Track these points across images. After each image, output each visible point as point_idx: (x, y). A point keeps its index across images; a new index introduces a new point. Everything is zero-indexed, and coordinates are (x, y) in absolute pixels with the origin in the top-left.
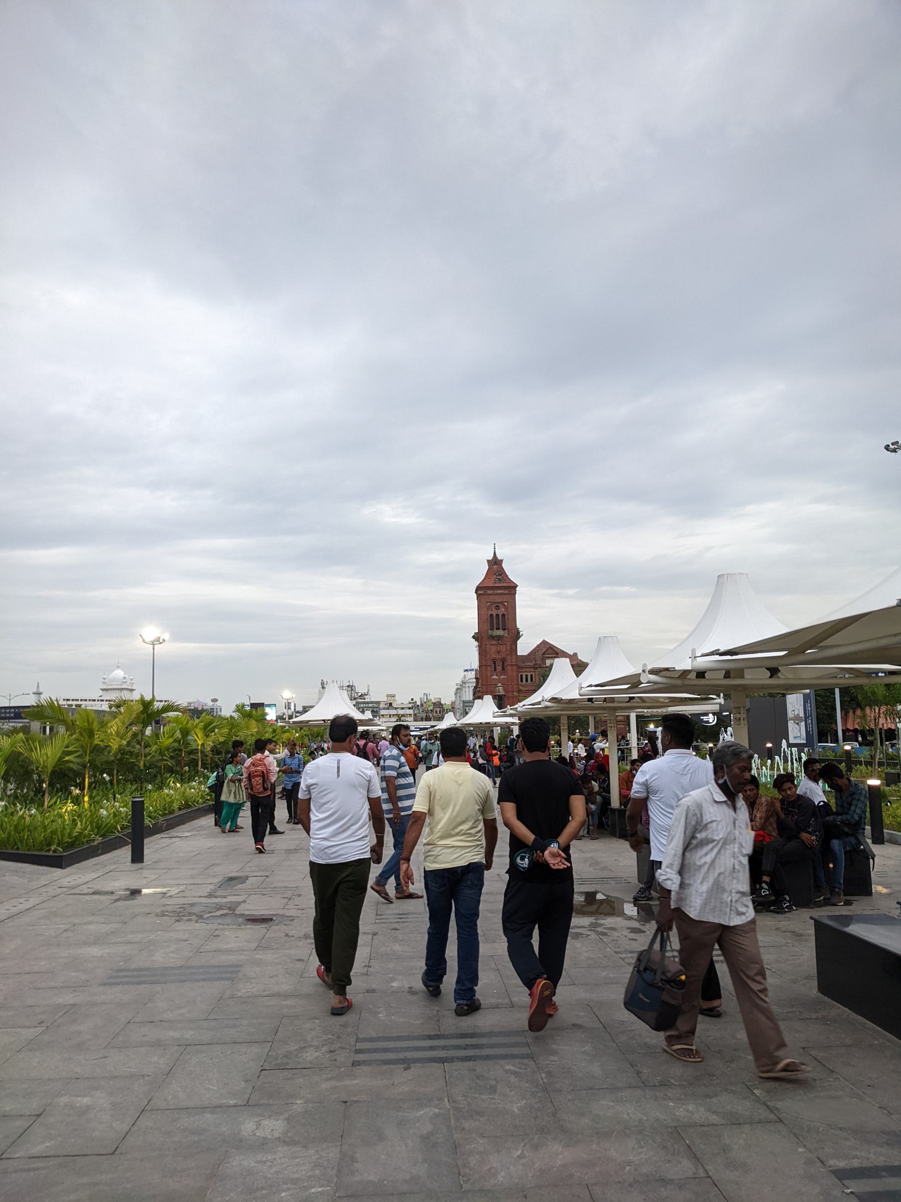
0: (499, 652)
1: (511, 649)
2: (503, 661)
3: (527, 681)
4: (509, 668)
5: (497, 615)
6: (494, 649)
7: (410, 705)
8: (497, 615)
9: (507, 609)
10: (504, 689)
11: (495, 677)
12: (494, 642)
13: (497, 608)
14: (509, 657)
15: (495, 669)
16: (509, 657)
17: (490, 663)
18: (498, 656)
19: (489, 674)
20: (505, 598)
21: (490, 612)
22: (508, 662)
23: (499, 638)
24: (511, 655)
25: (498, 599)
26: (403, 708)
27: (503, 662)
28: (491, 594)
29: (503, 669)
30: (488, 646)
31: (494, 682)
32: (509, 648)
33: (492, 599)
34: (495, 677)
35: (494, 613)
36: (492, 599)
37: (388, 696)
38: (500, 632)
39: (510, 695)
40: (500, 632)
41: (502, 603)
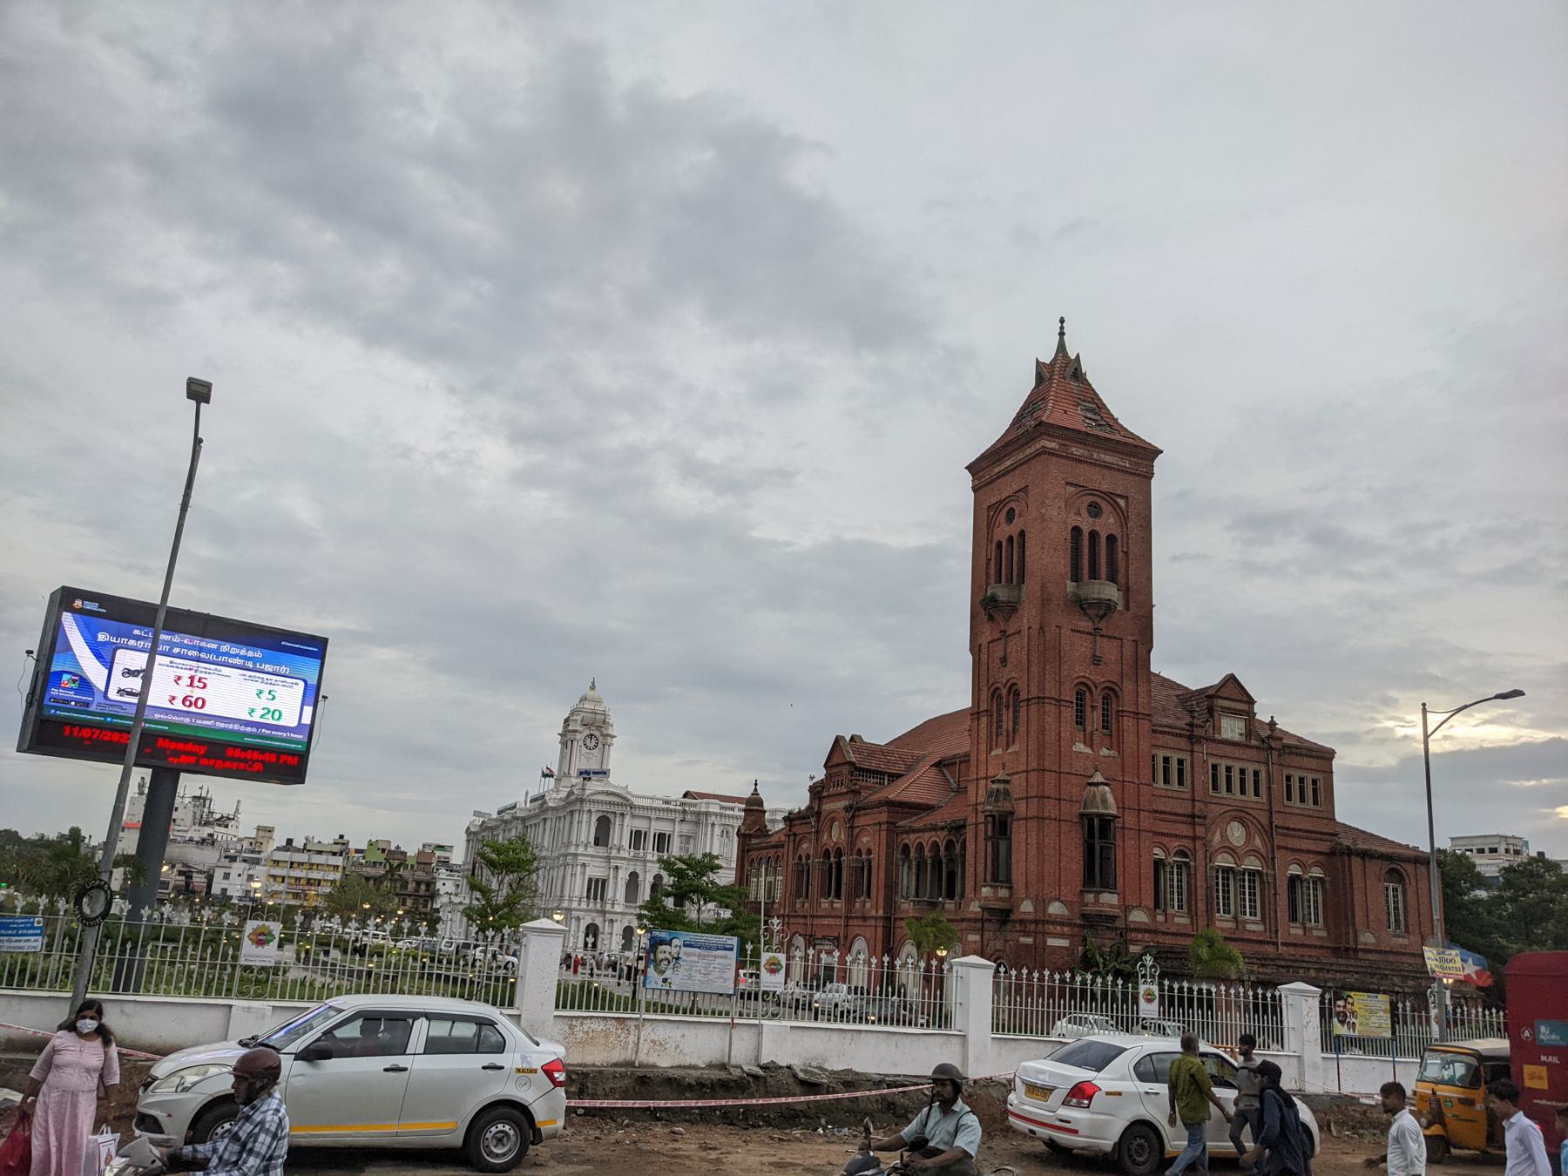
2: (1111, 693)
5: (1093, 535)
7: (337, 848)
9: (1123, 518)
11: (1080, 747)
12: (1085, 625)
16: (1128, 686)
18: (1098, 676)
19: (1066, 735)
26: (320, 852)
30: (1066, 632)
33: (1084, 474)
35: (1086, 524)
37: (259, 828)
38: (1111, 592)
40: (1111, 592)
41: (1110, 497)
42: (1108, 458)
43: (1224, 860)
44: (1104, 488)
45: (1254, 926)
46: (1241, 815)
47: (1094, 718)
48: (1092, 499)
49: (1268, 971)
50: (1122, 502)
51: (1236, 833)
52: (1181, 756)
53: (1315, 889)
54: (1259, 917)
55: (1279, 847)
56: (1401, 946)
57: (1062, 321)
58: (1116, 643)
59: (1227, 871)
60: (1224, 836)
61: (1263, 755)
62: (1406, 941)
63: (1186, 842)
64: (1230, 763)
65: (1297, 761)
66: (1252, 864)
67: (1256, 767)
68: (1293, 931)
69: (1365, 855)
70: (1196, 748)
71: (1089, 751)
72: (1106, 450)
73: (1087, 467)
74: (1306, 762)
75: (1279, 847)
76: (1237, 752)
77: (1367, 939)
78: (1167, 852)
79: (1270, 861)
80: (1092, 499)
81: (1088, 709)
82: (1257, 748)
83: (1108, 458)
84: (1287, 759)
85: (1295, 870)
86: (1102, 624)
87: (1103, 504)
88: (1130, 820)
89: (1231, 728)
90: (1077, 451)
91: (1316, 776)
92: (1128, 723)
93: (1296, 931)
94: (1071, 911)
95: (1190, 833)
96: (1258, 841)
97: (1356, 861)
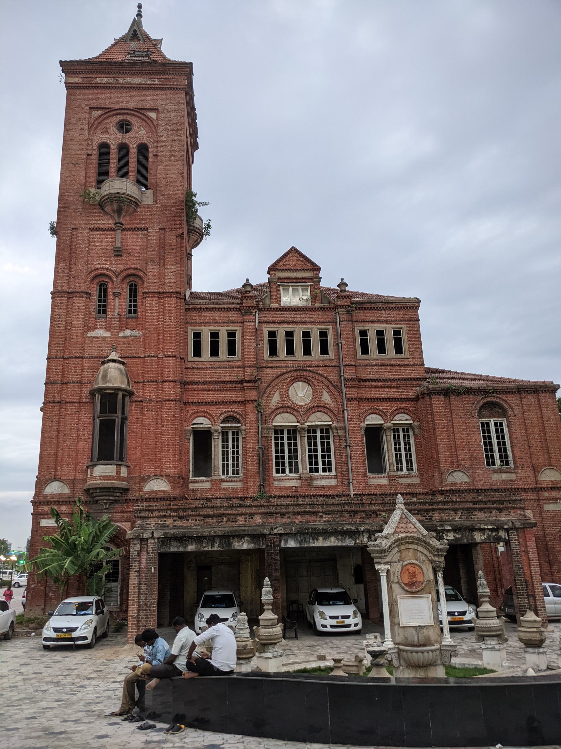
0: (118, 252)
1: (163, 245)
2: (134, 281)
3: (215, 352)
4: (151, 303)
5: (123, 148)
6: (103, 242)
8: (123, 148)
9: (153, 126)
10: (128, 375)
11: (100, 333)
12: (106, 222)
13: (124, 127)
14: (153, 269)
15: (102, 308)
16: (153, 269)
17: (82, 284)
20: (149, 99)
21: (99, 138)
22: (151, 283)
23: (121, 204)
24: (161, 260)
25: (131, 101)
27: (133, 289)
28: (104, 87)
29: (133, 308)
30: (83, 233)
31: (92, 350)
32: (154, 237)
34: (100, 333)
35: (114, 139)
36: (110, 99)
38: (126, 186)
39: (150, 392)
40: (126, 186)
41: (140, 112)
42: (136, 81)
43: (284, 420)
44: (132, 105)
45: (324, 481)
46: (302, 374)
47: (117, 305)
48: (120, 117)
49: (191, 522)
50: (153, 115)
51: (301, 393)
52: (232, 328)
53: (406, 437)
54: (334, 473)
55: (348, 399)
56: (505, 482)
57: (140, 6)
58: (140, 234)
59: (293, 431)
60: (285, 395)
61: (329, 315)
62: (513, 477)
63: (235, 408)
64: (289, 328)
65: (371, 315)
66: (319, 419)
67: (323, 327)
68: (373, 482)
69: (447, 392)
70: (247, 318)
71: (108, 334)
72: (134, 74)
73: (113, 92)
74: (384, 314)
75: (348, 399)
76: (299, 316)
77: (458, 479)
78: (213, 421)
79: (338, 415)
80: (120, 117)
81: (110, 296)
82: (322, 309)
83: (136, 80)
84: (359, 315)
85: (374, 420)
86: (125, 220)
87: (133, 120)
88: (139, 393)
89: (293, 296)
90: (100, 80)
91: (397, 326)
92: (151, 303)
93: (378, 481)
94: (73, 489)
95: (241, 399)
96: (326, 397)
97: (438, 401)
